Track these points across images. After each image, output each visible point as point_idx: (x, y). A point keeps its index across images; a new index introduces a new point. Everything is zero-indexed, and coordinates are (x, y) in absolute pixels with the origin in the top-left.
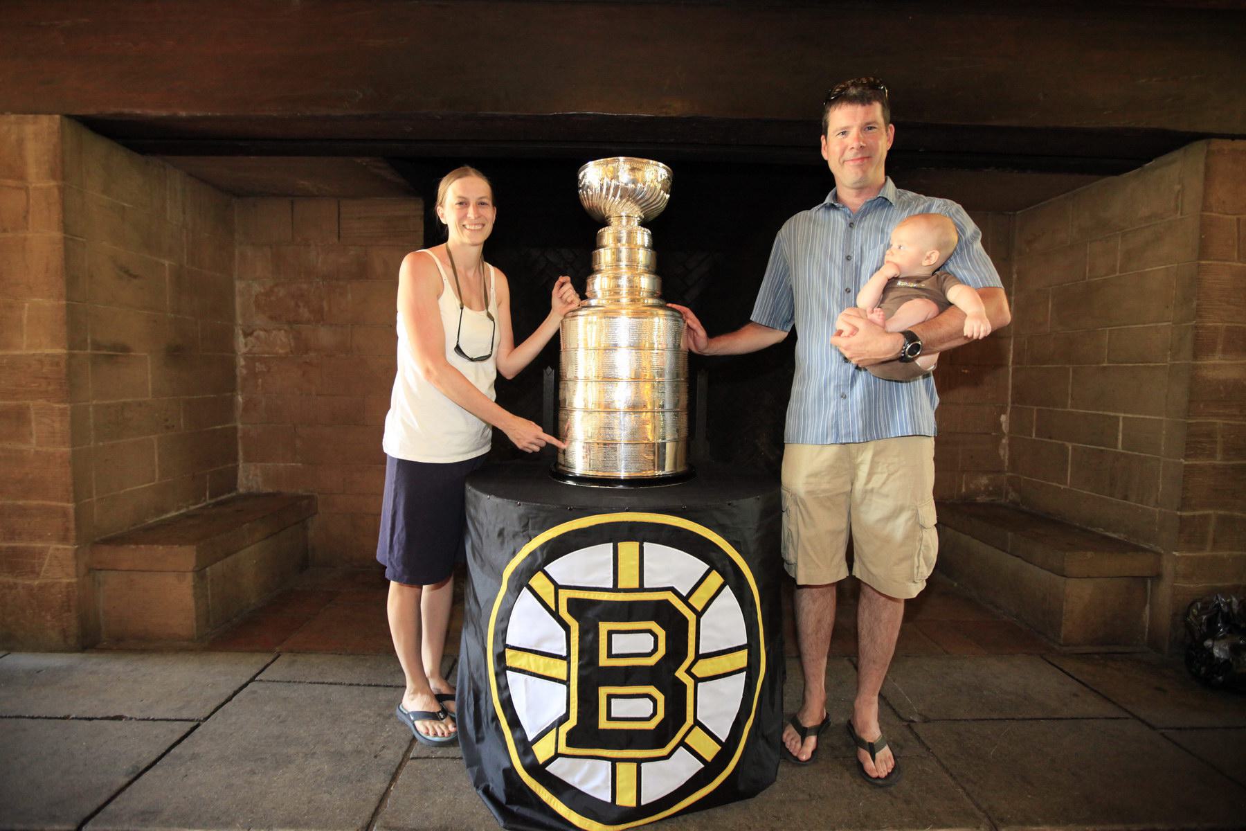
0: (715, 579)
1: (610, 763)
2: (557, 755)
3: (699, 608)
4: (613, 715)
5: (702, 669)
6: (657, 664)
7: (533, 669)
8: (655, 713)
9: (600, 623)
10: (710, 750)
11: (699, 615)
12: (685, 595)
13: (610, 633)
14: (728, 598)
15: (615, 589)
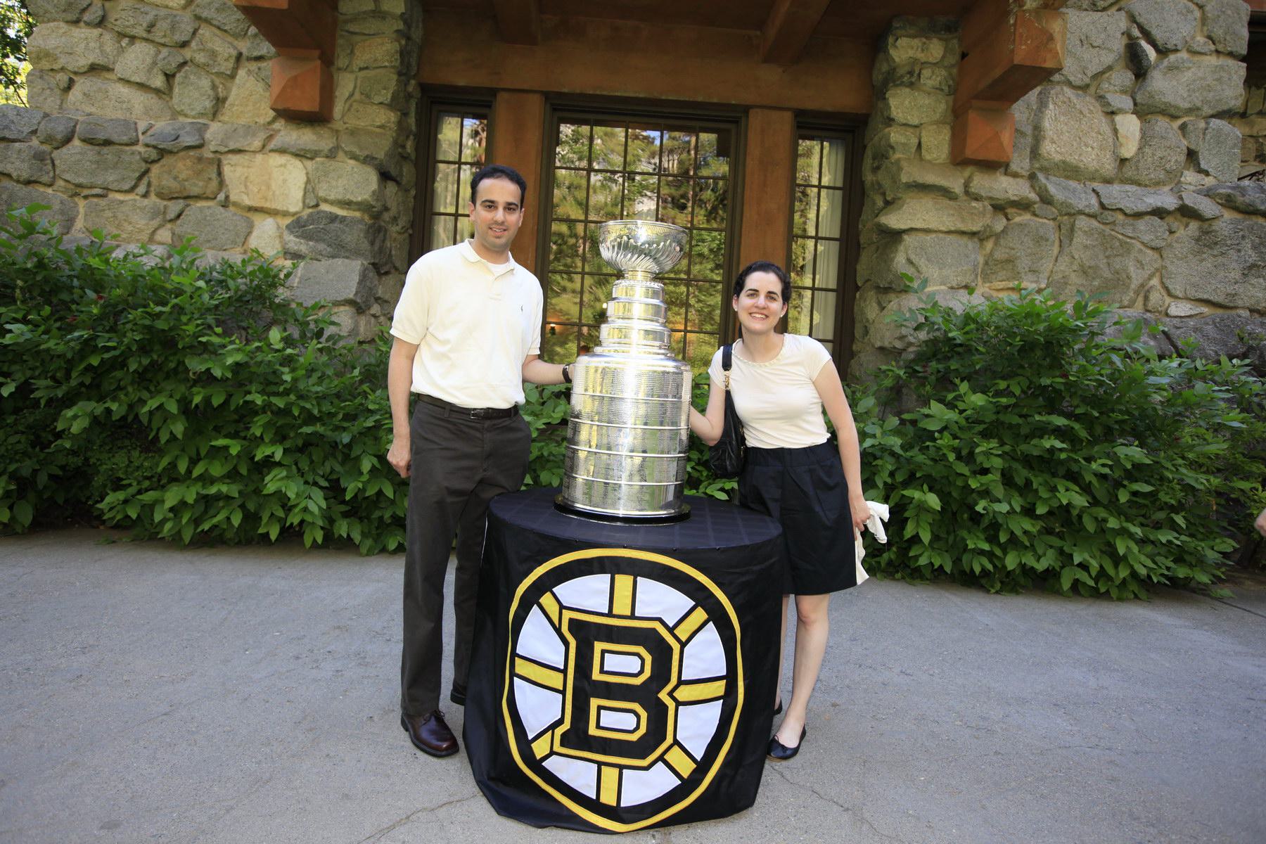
0: (701, 614)
1: (595, 766)
2: (552, 753)
3: (684, 639)
4: (602, 724)
5: (684, 693)
6: (644, 683)
7: (533, 679)
8: (638, 727)
9: (596, 644)
10: (686, 768)
11: (683, 645)
12: (671, 625)
13: (603, 652)
14: (711, 634)
15: (610, 614)
